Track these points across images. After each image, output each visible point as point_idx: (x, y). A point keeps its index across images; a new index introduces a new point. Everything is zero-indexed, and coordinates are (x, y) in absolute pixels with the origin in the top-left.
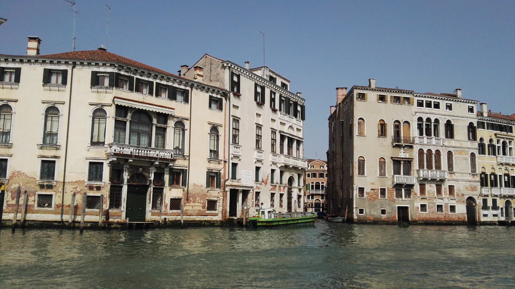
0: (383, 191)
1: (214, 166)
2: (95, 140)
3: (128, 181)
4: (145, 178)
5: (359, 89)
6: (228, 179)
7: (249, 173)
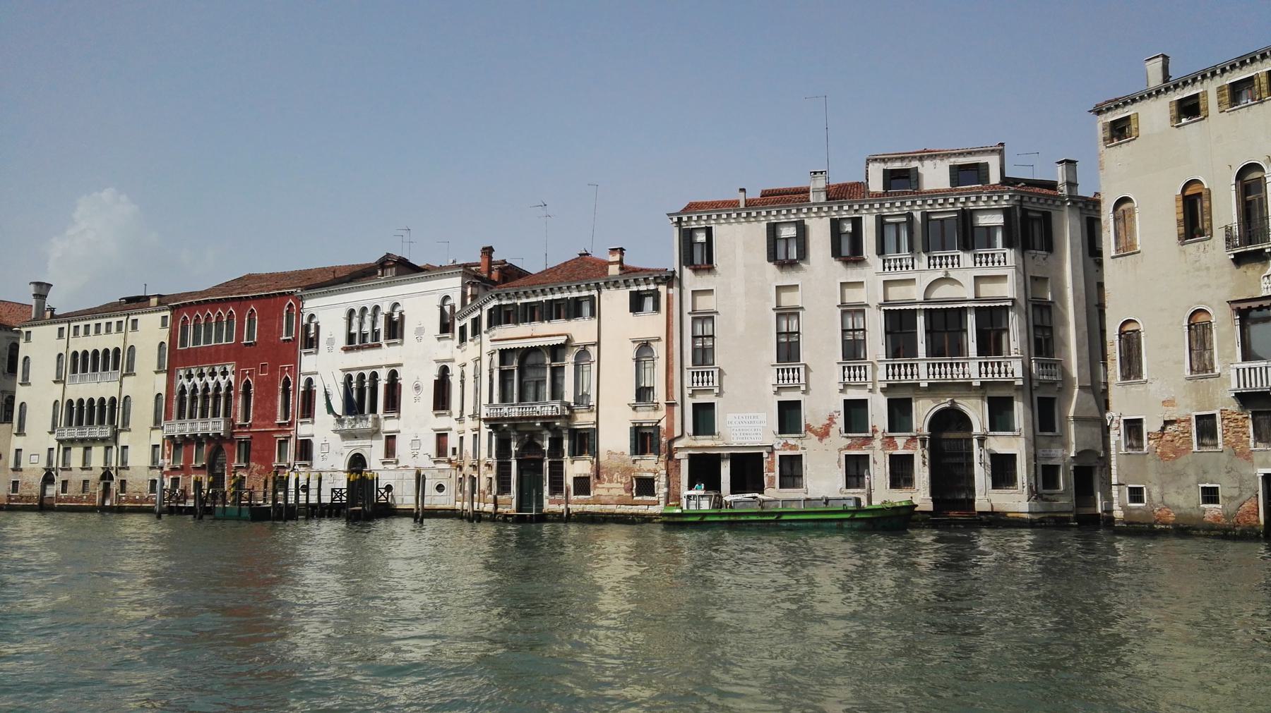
0: (1206, 426)
1: (646, 416)
4: (539, 447)
5: (1109, 109)
6: (682, 436)
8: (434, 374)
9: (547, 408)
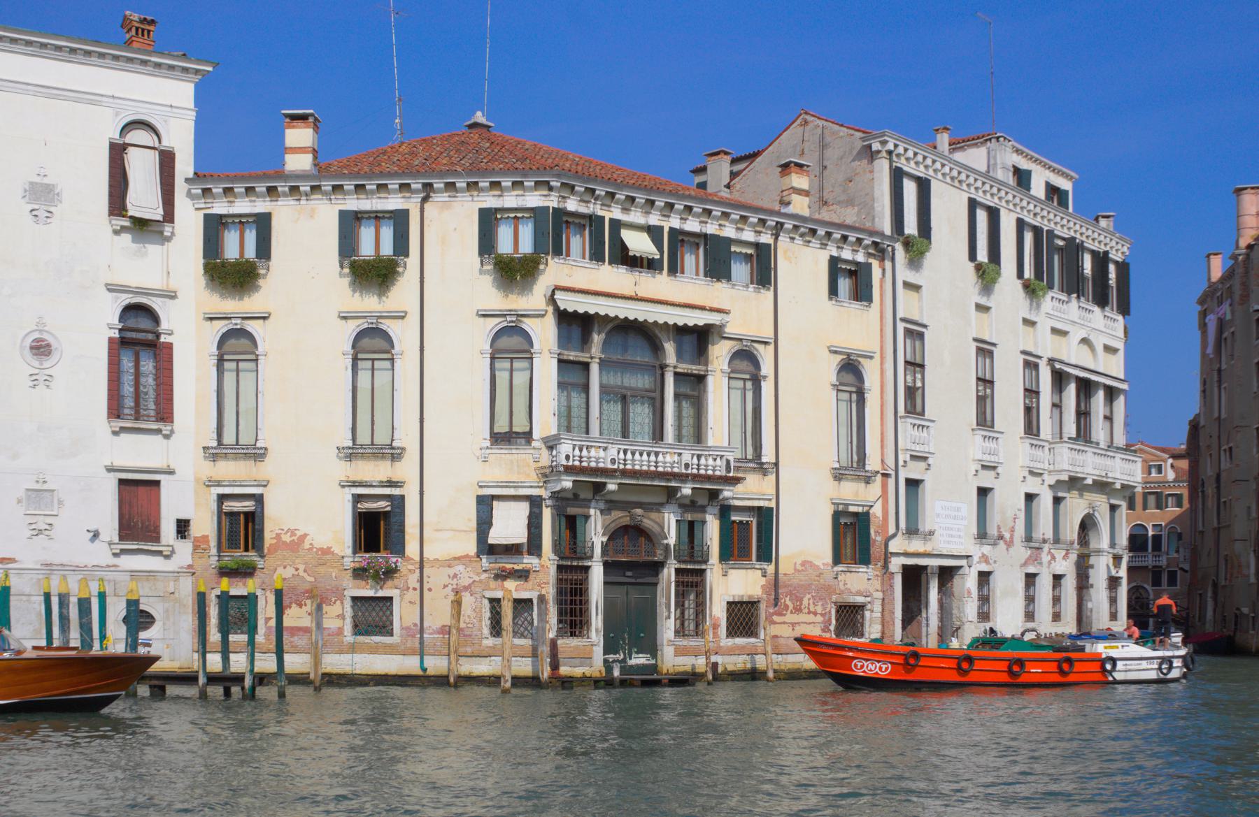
1: (855, 494)
2: (502, 426)
3: (605, 548)
6: (894, 536)
7: (959, 509)
8: (105, 318)
9: (671, 458)
